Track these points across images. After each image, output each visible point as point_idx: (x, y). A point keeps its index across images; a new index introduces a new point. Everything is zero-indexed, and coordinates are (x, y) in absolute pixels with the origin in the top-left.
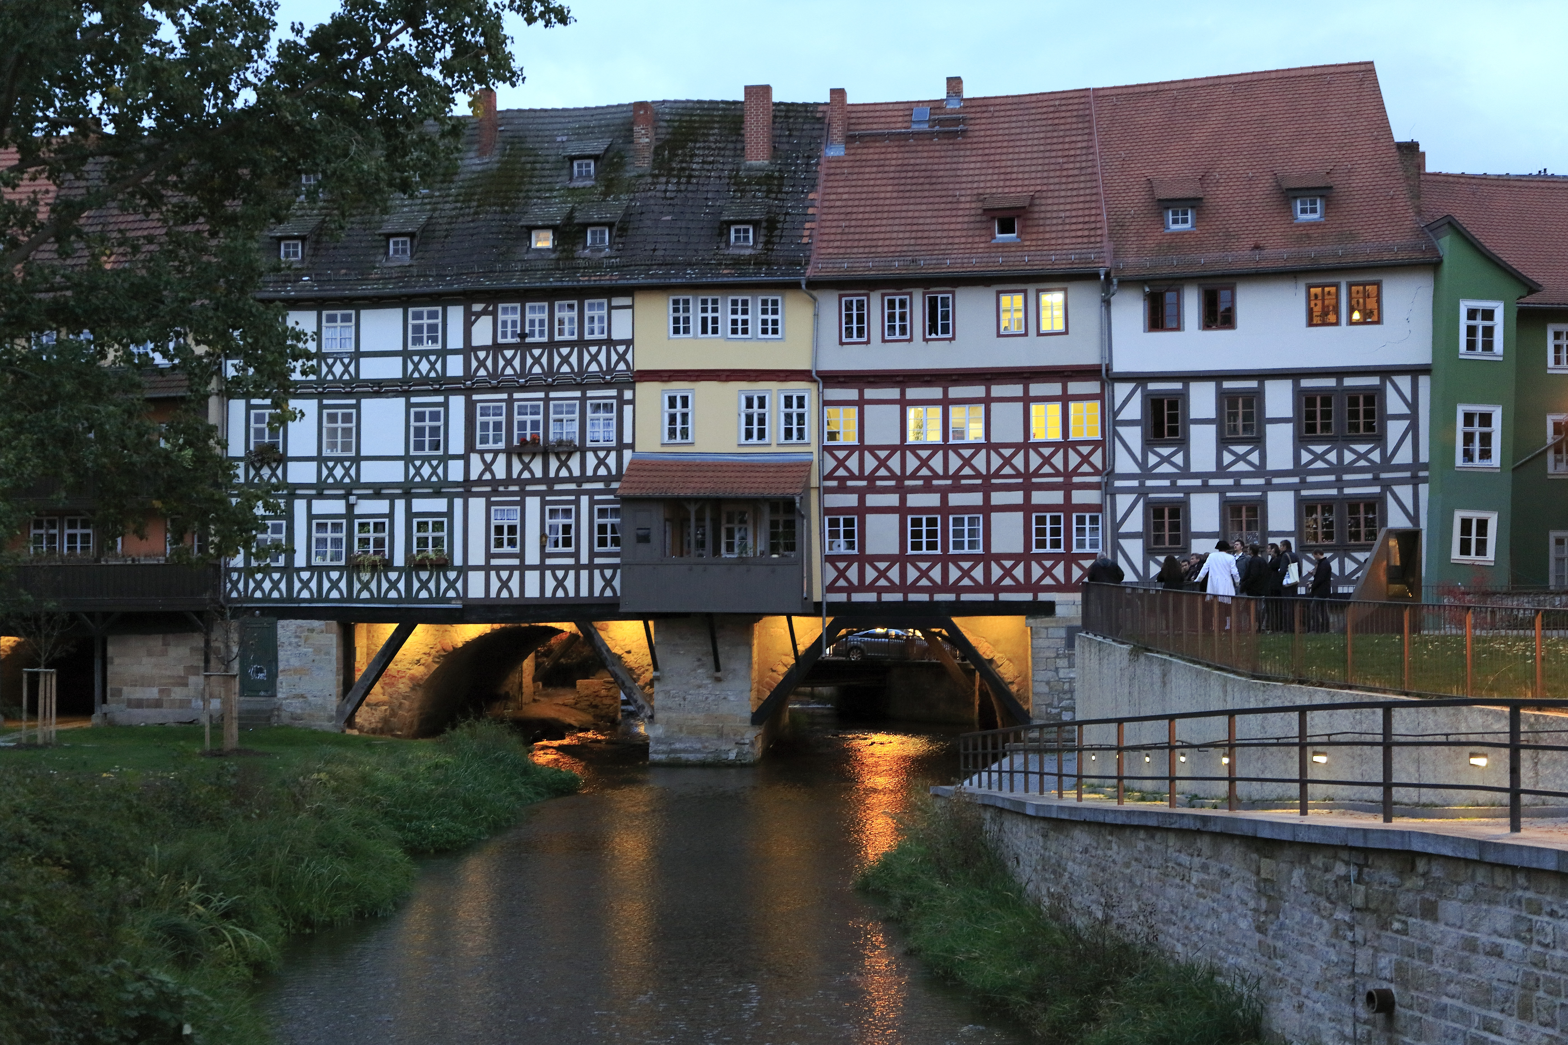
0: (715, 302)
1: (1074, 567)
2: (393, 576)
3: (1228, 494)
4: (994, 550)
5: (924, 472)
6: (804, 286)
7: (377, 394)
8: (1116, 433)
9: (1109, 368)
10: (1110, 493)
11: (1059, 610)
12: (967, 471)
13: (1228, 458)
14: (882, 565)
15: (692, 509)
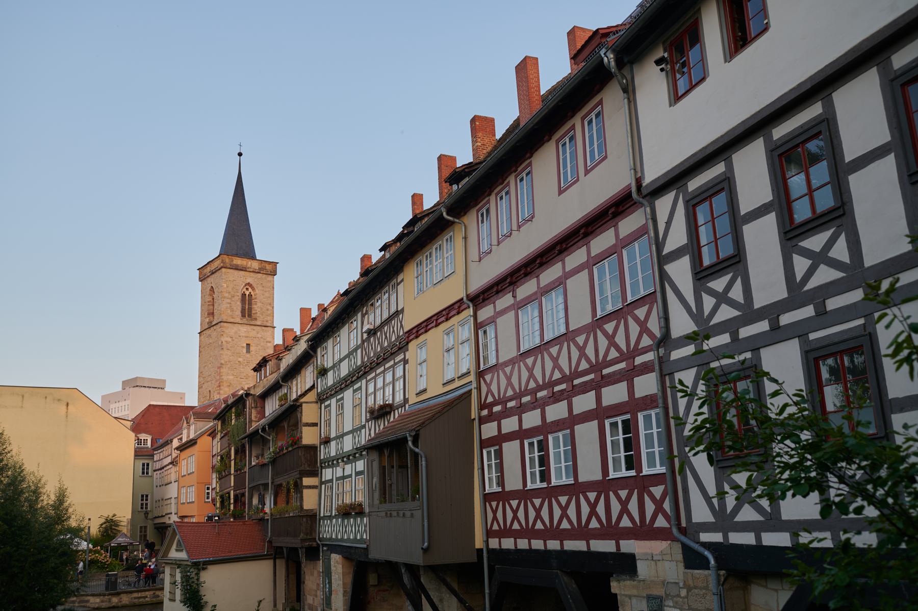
0: (430, 254)
1: (647, 499)
2: (352, 520)
3: (813, 336)
4: (582, 478)
5: (532, 385)
6: (445, 214)
7: (347, 387)
8: (664, 277)
9: (639, 181)
10: (665, 370)
11: (641, 567)
12: (557, 375)
13: (801, 265)
14: (514, 503)
15: (386, 453)
